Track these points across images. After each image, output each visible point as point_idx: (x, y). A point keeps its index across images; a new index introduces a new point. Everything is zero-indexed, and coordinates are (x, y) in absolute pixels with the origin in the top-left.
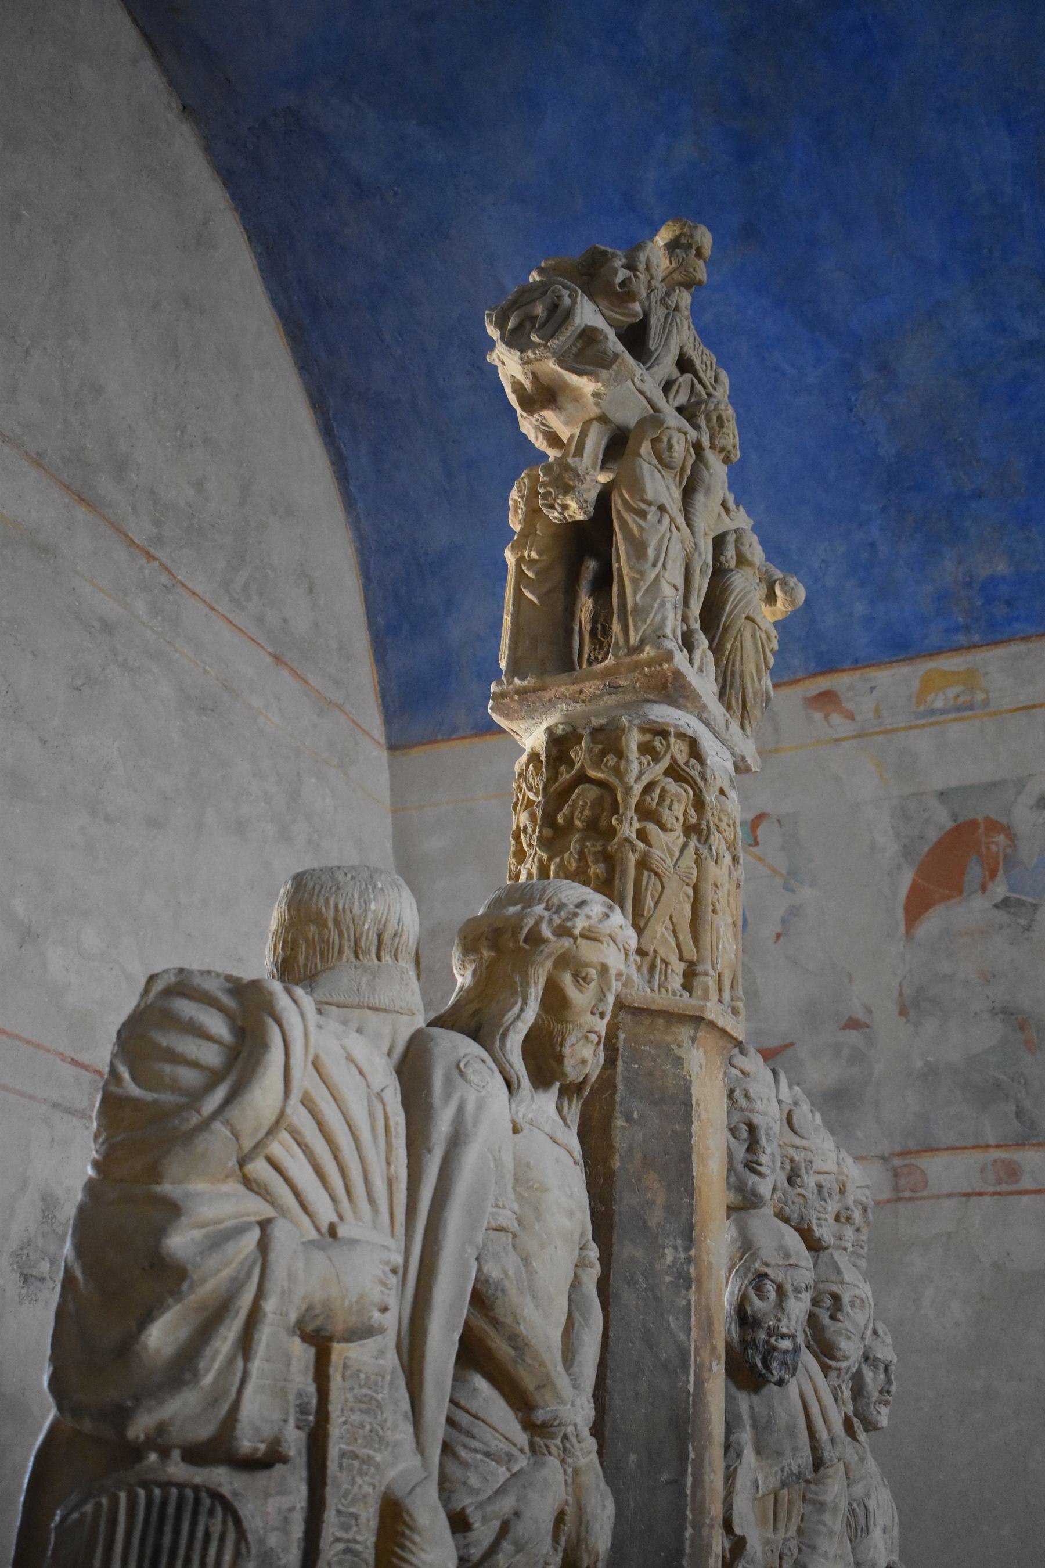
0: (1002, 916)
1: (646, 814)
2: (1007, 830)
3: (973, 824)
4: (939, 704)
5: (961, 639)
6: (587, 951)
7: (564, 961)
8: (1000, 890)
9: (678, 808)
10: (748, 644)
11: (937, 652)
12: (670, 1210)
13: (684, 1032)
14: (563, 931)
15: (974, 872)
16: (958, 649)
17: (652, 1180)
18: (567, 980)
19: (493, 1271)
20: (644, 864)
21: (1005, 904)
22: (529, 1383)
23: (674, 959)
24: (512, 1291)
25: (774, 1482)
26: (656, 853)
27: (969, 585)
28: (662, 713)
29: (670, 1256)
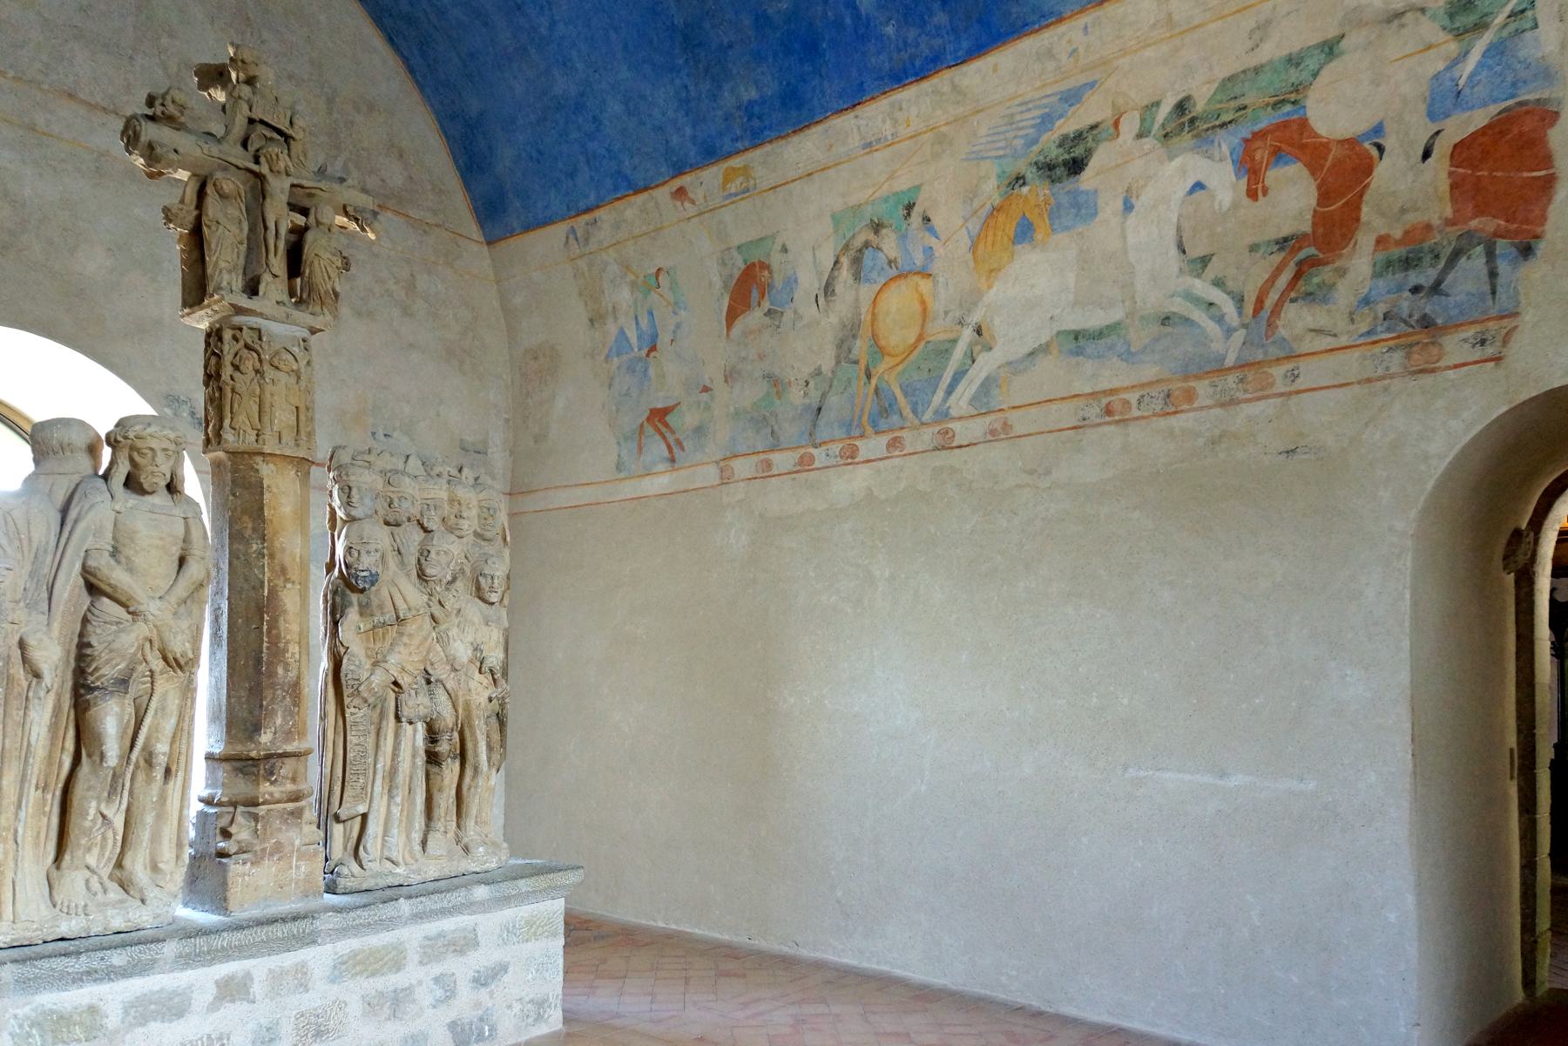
0: (767, 320)
1: (236, 368)
2: (768, 267)
3: (753, 264)
4: (733, 190)
5: (739, 145)
6: (139, 444)
7: (132, 448)
8: (766, 305)
9: (250, 363)
10: (317, 269)
11: (729, 155)
12: (254, 530)
13: (259, 459)
14: (126, 438)
15: (755, 294)
16: (738, 152)
17: (246, 518)
18: (135, 455)
19: (91, 563)
20: (233, 391)
21: (769, 313)
22: (124, 599)
23: (249, 430)
24: (105, 571)
25: (369, 626)
26: (238, 386)
27: (739, 108)
28: (239, 320)
29: (255, 547)
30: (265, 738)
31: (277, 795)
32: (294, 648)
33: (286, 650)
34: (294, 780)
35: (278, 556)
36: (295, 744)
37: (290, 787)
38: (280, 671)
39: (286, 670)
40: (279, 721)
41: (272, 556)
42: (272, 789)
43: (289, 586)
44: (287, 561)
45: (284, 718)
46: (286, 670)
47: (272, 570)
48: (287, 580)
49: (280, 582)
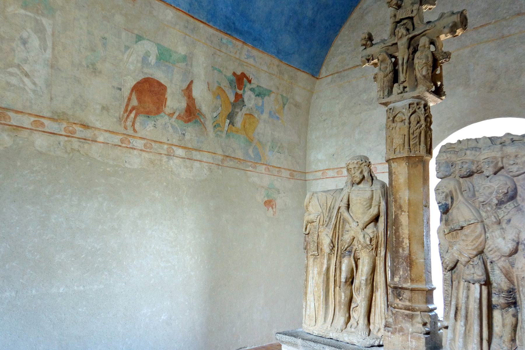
30: (396, 279)
31: (400, 306)
32: (406, 241)
33: (403, 242)
34: (410, 301)
35: (398, 201)
36: (409, 284)
37: (408, 303)
38: (401, 251)
39: (403, 250)
40: (401, 273)
41: (396, 201)
42: (400, 302)
43: (403, 213)
44: (402, 202)
45: (403, 271)
46: (403, 250)
47: (396, 207)
48: (402, 211)
49: (399, 212)
